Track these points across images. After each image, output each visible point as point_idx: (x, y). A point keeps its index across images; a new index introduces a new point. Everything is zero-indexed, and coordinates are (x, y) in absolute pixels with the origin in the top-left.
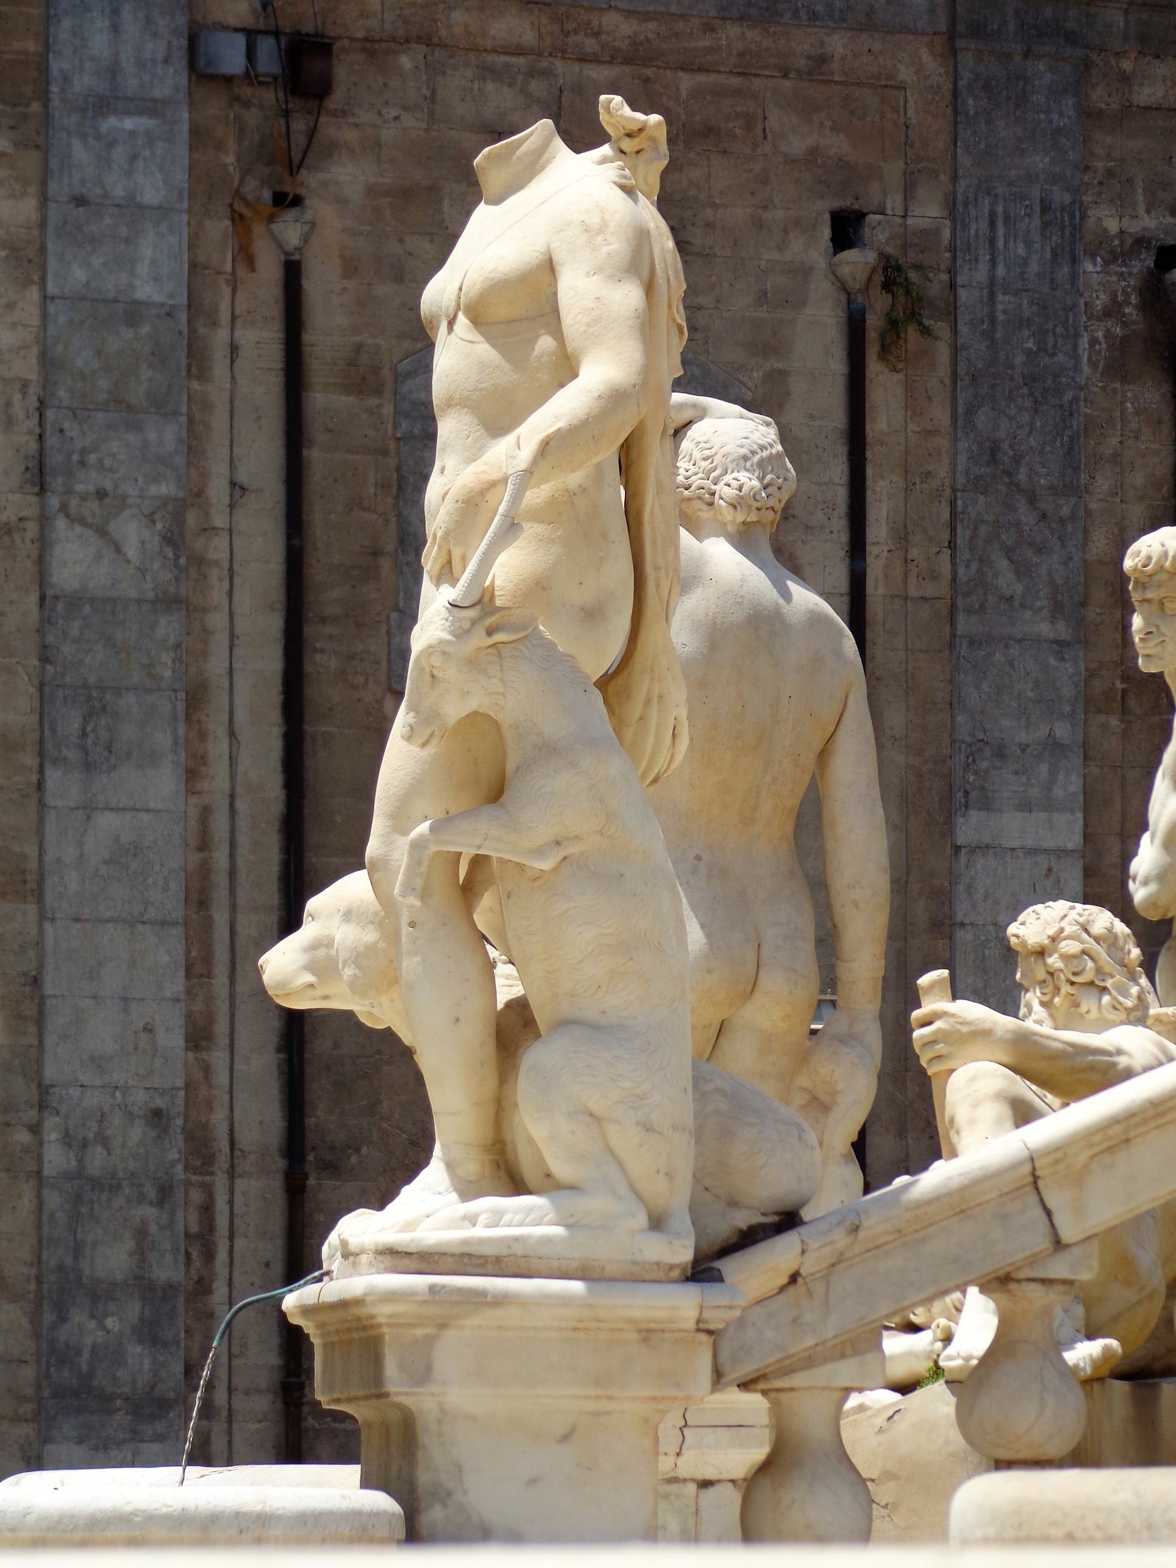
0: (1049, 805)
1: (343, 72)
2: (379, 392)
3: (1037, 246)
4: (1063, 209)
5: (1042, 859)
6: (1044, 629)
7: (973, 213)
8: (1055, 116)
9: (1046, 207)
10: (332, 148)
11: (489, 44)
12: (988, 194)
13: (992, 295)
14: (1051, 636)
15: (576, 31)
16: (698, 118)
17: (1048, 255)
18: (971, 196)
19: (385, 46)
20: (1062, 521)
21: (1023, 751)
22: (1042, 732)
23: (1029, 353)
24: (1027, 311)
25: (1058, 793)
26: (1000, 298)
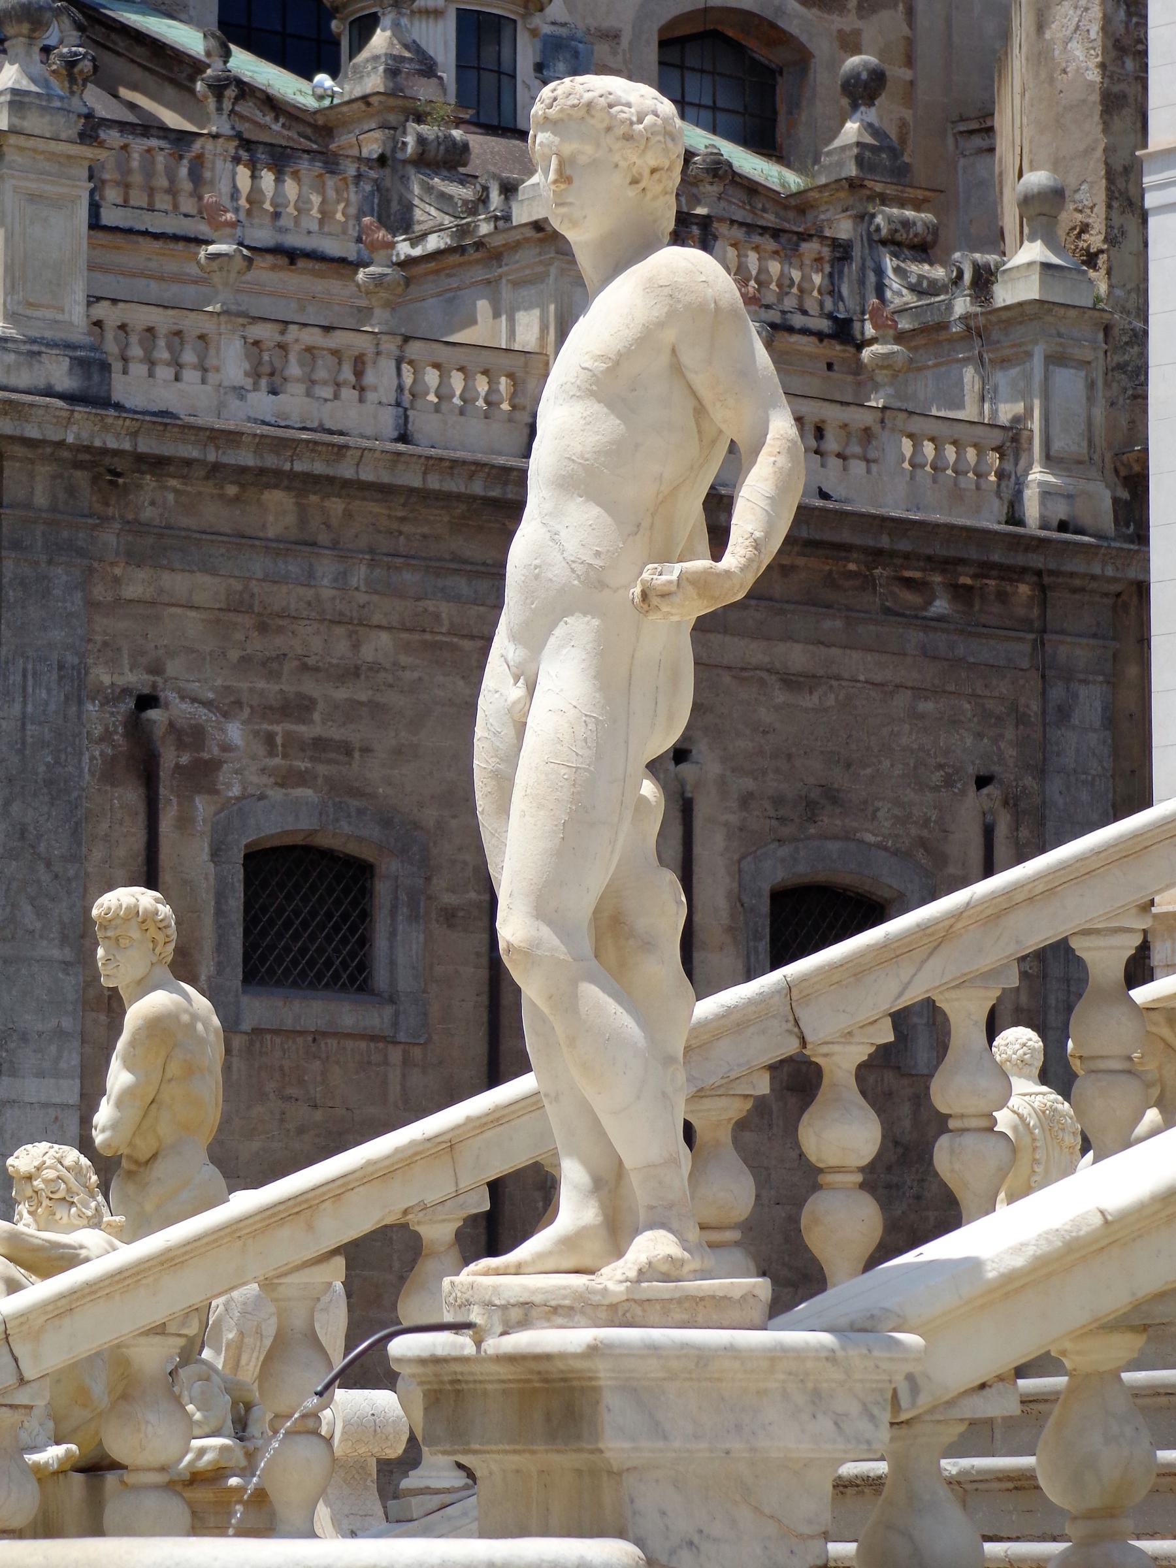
0: (57, 1074)
3: (55, 692)
4: (73, 668)
5: (52, 1112)
6: (56, 953)
7: (11, 670)
8: (68, 605)
9: (61, 667)
12: (22, 656)
13: (23, 725)
14: (60, 958)
17: (62, 698)
18: (10, 657)
20: (69, 879)
21: (40, 1036)
22: (53, 1023)
23: (48, 765)
24: (48, 736)
25: (63, 1065)
26: (29, 727)
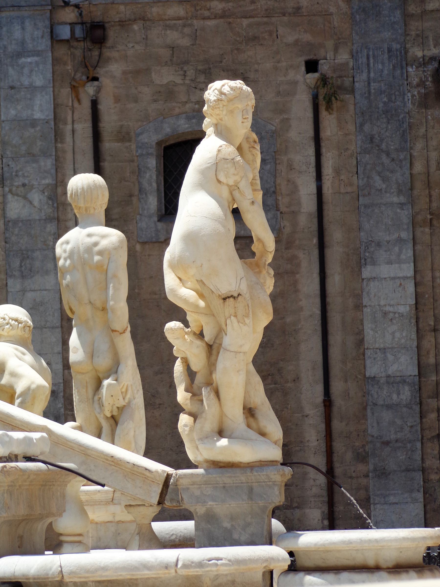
0: (400, 262)
1: (112, 34)
2: (130, 141)
3: (387, 65)
4: (397, 50)
5: (398, 282)
6: (395, 199)
7: (360, 55)
8: (392, 18)
9: (390, 50)
10: (108, 60)
11: (167, 17)
12: (366, 48)
13: (369, 83)
14: (398, 201)
15: (200, 9)
16: (250, 34)
17: (391, 67)
18: (359, 50)
19: (127, 23)
20: (401, 161)
21: (388, 243)
22: (396, 235)
23: (385, 103)
24: (383, 88)
25: (403, 257)
26: (372, 84)
